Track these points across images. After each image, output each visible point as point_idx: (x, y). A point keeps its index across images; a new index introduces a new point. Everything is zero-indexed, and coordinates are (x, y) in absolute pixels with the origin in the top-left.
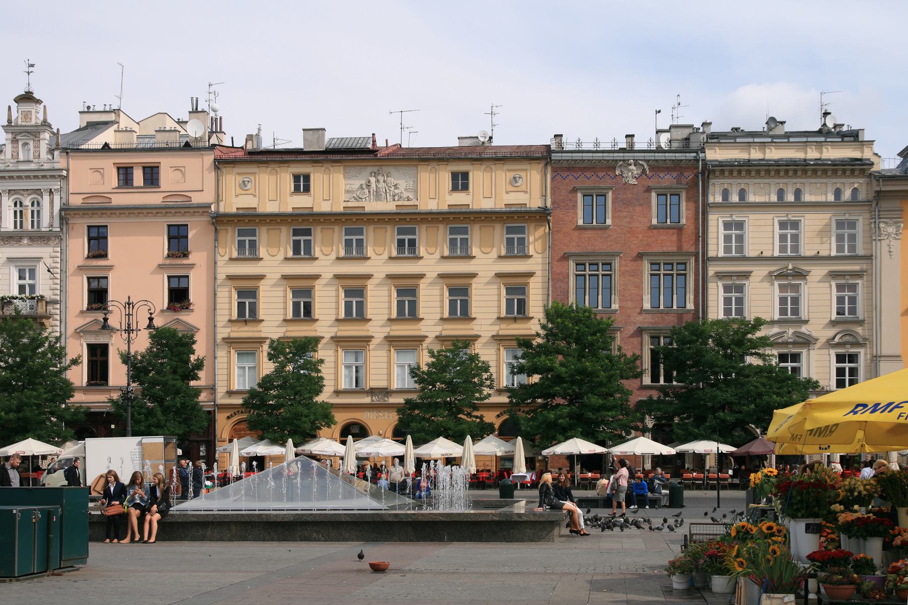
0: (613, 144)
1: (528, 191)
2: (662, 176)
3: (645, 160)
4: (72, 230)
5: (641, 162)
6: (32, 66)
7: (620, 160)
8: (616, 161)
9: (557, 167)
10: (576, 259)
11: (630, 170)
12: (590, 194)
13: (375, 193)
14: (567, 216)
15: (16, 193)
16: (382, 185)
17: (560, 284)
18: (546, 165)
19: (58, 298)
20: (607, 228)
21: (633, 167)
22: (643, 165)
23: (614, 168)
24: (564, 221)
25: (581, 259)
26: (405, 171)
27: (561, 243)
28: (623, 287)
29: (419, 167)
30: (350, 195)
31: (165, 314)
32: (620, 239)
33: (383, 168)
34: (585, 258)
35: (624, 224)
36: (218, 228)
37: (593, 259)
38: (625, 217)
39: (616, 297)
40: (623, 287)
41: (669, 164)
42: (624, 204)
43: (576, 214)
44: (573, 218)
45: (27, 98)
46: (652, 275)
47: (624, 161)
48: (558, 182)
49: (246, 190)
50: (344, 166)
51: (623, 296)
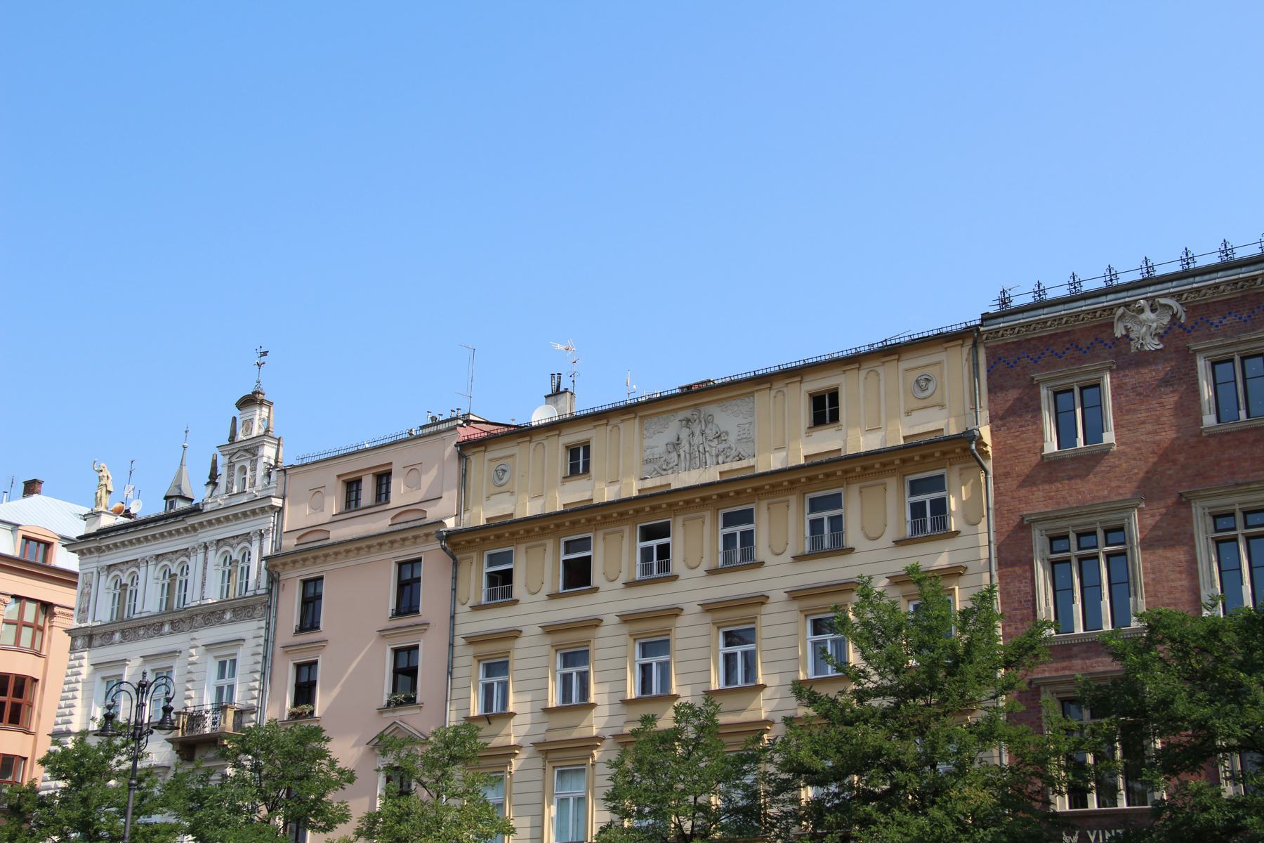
0: (1108, 279)
1: (947, 403)
2: (1216, 321)
3: (1172, 295)
4: (283, 590)
5: (1163, 301)
6: (265, 354)
7: (1119, 306)
8: (1111, 308)
9: (998, 346)
10: (1047, 526)
11: (1141, 323)
12: (1067, 387)
13: (688, 456)
14: (1022, 440)
15: (225, 544)
16: (698, 439)
17: (1017, 584)
18: (975, 345)
19: (255, 702)
20: (1106, 451)
21: (1148, 315)
22: (1170, 307)
23: (1111, 325)
24: (1017, 451)
25: (1057, 526)
26: (736, 408)
27: (1013, 498)
28: (1152, 576)
29: (756, 395)
30: (649, 467)
31: (385, 715)
32: (1136, 471)
33: (702, 408)
34: (1064, 523)
35: (1142, 437)
36: (458, 557)
37: (1083, 523)
38: (1143, 423)
39: (1139, 600)
40: (1152, 576)
41: (1228, 293)
42: (1140, 394)
43: (1042, 433)
44: (1035, 442)
45: (248, 402)
46: (1218, 542)
47: (1127, 305)
48: (1000, 376)
49: (501, 486)
50: (641, 417)
51: (1156, 596)
